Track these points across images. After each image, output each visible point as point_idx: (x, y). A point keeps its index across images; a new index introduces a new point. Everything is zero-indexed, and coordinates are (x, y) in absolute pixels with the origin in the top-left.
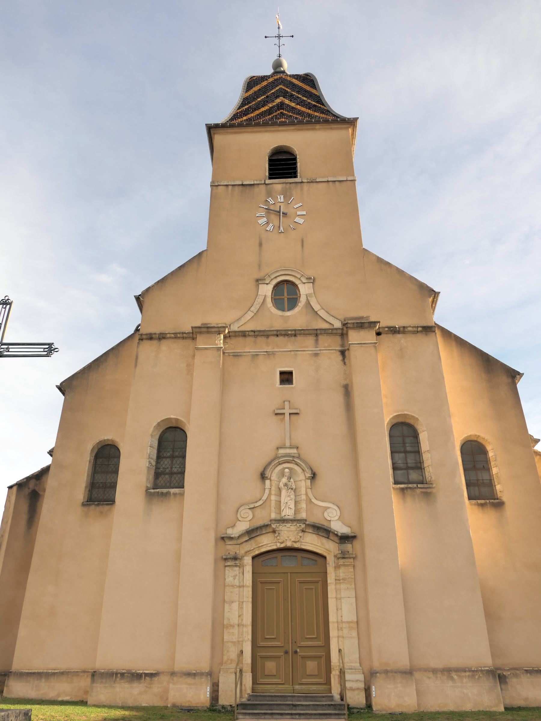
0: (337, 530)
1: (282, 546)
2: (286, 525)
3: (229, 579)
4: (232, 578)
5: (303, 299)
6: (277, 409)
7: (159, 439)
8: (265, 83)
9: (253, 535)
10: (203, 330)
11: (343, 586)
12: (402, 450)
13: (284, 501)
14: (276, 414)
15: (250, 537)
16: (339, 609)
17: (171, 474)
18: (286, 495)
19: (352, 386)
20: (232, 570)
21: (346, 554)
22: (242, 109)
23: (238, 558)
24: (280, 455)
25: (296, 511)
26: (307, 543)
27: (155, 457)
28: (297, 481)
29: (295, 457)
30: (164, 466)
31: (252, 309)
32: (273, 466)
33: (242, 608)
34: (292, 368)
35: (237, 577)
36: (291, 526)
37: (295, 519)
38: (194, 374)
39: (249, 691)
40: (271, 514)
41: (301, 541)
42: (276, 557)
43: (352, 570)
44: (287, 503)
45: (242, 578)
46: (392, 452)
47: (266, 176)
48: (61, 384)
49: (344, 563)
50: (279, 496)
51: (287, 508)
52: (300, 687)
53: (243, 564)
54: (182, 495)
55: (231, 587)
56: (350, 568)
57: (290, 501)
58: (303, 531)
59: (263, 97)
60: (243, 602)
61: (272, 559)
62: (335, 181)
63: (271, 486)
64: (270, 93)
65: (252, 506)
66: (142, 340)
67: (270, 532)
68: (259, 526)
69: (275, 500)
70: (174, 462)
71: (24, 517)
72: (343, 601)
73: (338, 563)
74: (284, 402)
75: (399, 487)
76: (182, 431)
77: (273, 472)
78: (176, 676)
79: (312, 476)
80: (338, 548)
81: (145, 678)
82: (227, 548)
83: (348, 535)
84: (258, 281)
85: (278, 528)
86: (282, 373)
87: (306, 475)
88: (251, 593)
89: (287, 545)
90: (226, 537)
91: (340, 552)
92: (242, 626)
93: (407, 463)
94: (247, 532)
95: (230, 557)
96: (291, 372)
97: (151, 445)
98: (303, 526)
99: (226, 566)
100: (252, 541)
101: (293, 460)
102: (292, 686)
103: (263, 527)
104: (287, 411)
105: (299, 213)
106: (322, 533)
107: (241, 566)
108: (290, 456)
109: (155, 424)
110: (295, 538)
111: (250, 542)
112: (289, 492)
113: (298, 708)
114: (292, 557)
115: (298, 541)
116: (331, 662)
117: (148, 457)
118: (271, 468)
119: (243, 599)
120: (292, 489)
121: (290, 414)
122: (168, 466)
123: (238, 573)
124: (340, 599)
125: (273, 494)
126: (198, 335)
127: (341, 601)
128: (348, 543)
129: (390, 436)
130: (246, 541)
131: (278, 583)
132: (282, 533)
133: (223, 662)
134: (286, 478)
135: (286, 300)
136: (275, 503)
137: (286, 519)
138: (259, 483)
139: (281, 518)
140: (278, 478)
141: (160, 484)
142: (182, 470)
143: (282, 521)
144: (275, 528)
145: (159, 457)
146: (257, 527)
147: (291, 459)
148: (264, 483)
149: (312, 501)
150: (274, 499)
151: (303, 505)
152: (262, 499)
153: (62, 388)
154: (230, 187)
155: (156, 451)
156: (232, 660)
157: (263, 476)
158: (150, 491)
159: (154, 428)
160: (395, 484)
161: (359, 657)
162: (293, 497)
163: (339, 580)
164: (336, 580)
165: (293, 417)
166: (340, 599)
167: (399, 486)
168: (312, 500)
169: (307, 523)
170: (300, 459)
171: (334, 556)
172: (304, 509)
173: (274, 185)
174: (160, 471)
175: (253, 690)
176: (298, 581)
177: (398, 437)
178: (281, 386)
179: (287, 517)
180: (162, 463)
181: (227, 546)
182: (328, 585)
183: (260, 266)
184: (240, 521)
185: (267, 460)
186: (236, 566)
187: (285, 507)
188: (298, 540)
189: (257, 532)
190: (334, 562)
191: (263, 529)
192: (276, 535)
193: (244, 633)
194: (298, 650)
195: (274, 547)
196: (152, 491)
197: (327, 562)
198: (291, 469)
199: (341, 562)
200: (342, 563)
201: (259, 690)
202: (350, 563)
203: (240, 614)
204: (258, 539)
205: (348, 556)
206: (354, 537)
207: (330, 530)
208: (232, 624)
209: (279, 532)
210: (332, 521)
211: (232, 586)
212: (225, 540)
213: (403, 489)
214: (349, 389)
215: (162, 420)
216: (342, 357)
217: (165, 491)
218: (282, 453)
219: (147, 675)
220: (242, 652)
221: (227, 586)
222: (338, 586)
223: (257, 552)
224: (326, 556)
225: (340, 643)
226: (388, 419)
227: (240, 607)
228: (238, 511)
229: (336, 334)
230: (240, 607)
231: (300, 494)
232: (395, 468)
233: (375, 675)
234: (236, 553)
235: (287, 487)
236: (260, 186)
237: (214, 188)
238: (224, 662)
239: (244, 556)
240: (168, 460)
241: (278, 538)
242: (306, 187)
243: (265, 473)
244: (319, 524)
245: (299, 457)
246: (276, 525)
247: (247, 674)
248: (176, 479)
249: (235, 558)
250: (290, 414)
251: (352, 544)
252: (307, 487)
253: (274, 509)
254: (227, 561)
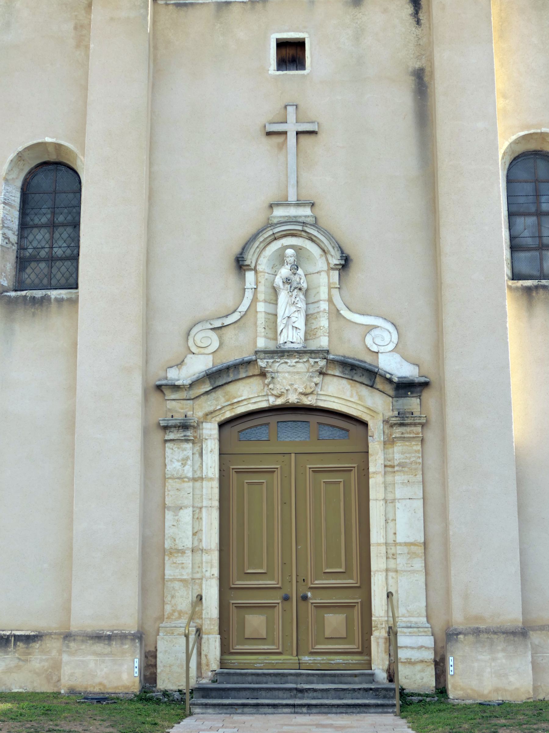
0: (390, 372)
1: (279, 402)
2: (286, 360)
3: (174, 465)
4: (180, 464)
6: (270, 123)
7: (22, 189)
11: (399, 478)
12: (533, 209)
13: (282, 314)
14: (269, 134)
15: (214, 386)
16: (389, 521)
17: (51, 259)
18: (287, 303)
19: (432, 73)
20: (178, 448)
21: (407, 417)
23: (191, 426)
24: (275, 221)
25: (309, 335)
26: (330, 396)
27: (15, 225)
28: (310, 274)
29: (308, 224)
30: (35, 244)
32: (261, 242)
33: (200, 519)
34: (303, 32)
35: (189, 462)
36: (296, 362)
37: (305, 349)
38: (92, 46)
39: (215, 666)
40: (258, 341)
41: (317, 392)
42: (268, 424)
43: (419, 448)
44: (289, 317)
45: (199, 463)
46: (511, 215)
49: (403, 433)
50: (273, 303)
51: (290, 327)
52: (312, 659)
53: (200, 436)
54: (74, 302)
55: (176, 480)
56: (413, 443)
57: (296, 314)
58: (321, 373)
60: (201, 508)
61: (259, 427)
63: (257, 284)
65: (218, 324)
67: (254, 376)
68: (231, 363)
69: (265, 312)
70: (57, 235)
72: (398, 505)
73: (391, 435)
74: (286, 107)
75: (522, 285)
76: (71, 172)
77: (262, 256)
78: (74, 640)
79: (343, 262)
80: (392, 407)
81: (15, 644)
82: (168, 407)
83: (414, 380)
85: (270, 367)
86: (281, 45)
87: (330, 261)
88: (216, 491)
89: (288, 399)
90: (166, 385)
91: (396, 413)
92: (200, 552)
93: (540, 237)
94: (207, 375)
95: (174, 424)
96: (301, 41)
97: (5, 199)
98: (322, 363)
99: (166, 441)
100: (219, 393)
101: (303, 231)
102: (297, 658)
103: (241, 366)
104: (291, 128)
106: (360, 376)
107: (198, 441)
108: (297, 222)
110: (306, 386)
111: (213, 395)
112: (294, 296)
113: (306, 694)
114: (299, 423)
115: (312, 393)
116: (373, 616)
117: (2, 225)
118: (258, 247)
119: (202, 502)
120: (300, 289)
121: (298, 133)
122: (43, 243)
123: (190, 454)
124: (392, 502)
125: (261, 300)
127: (395, 506)
128: (413, 397)
129: (510, 181)
130: (207, 393)
131: (271, 472)
132: (280, 378)
133: (164, 615)
134: (289, 267)
136: (265, 318)
137: (287, 349)
138: (232, 279)
139: (277, 348)
140: (272, 268)
141: (28, 281)
142: (72, 252)
143: (279, 354)
144: (265, 368)
145: (24, 226)
146: (229, 366)
147: (300, 228)
148: (243, 278)
149: (341, 314)
150: (263, 310)
151: (324, 322)
152: (239, 310)
155: (16, 214)
156: (180, 613)
157: (241, 263)
158: (8, 294)
159: (10, 163)
160: (513, 280)
161: (427, 606)
162: (302, 305)
163: (393, 467)
164: (385, 466)
165: (304, 139)
166: (393, 501)
167: (521, 283)
168: (342, 312)
169: (331, 357)
170: (317, 227)
171: (384, 421)
172: (324, 329)
174: (28, 254)
175: (222, 664)
176: (310, 468)
177: (526, 182)
178: (280, 72)
179: (289, 346)
180: (31, 237)
181: (168, 402)
182: (370, 476)
184: (194, 353)
185: (251, 230)
186: (187, 441)
187: (286, 325)
188: (312, 389)
189: (229, 376)
190: (384, 432)
191: (241, 370)
192: (267, 381)
193: (204, 564)
194: (309, 594)
195: (264, 405)
196: (13, 294)
197: (370, 433)
198: (298, 249)
199: (397, 432)
200: (398, 435)
201: (234, 663)
202: (416, 434)
203: (195, 531)
204: (231, 388)
205: (412, 421)
206: (425, 385)
207: (376, 370)
208: (180, 548)
209: (273, 376)
210: (382, 353)
211: (178, 478)
212: (164, 390)
213: (528, 290)
214: (426, 79)
215: (26, 148)
216: (412, 9)
217: (38, 294)
218: (281, 217)
219: (18, 638)
220: (200, 598)
221: (168, 478)
222: (389, 478)
223: (228, 414)
224: (367, 421)
225: (391, 581)
226: (507, 144)
227: (196, 516)
228: (188, 334)
230: (196, 516)
231: (316, 300)
232: (514, 248)
233: (455, 637)
234: (186, 416)
235: (289, 286)
238: (166, 616)
239: (202, 423)
240: (43, 231)
241: (271, 386)
243: (245, 256)
244: (354, 359)
245: (315, 225)
246: (267, 362)
247: (210, 636)
248: (61, 269)
249: (185, 426)
250: (298, 133)
251: (420, 399)
252: (332, 286)
253: (263, 330)
254: (168, 431)
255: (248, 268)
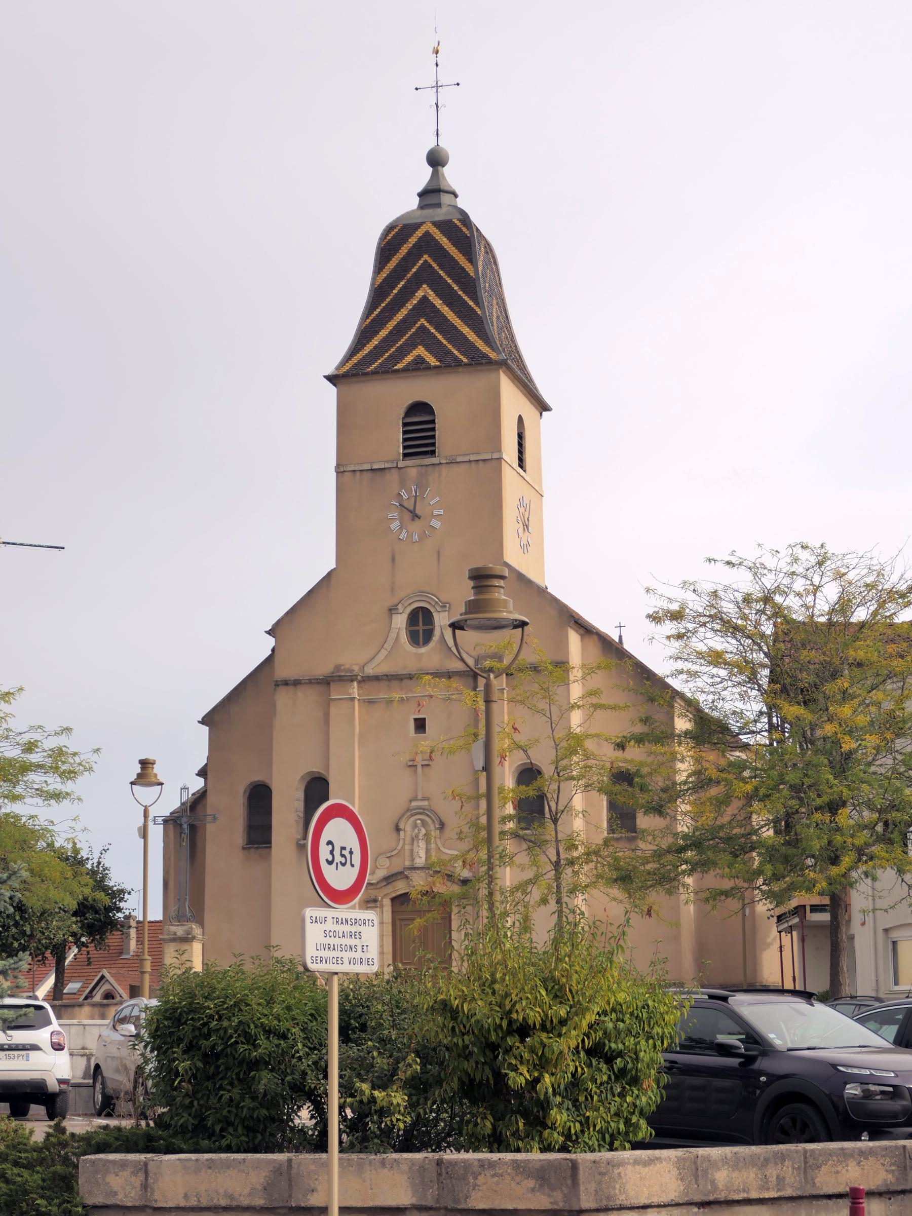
5: (437, 632)
8: (404, 250)
9: (390, 881)
10: (335, 678)
14: (410, 766)
22: (373, 315)
24: (411, 808)
31: (385, 646)
47: (399, 453)
48: (203, 718)
59: (402, 283)
62: (478, 461)
64: (411, 273)
65: (388, 855)
66: (278, 685)
71: (186, 852)
84: (392, 610)
86: (415, 720)
100: (390, 886)
105: (436, 512)
107: (382, 906)
108: (421, 809)
109: (299, 777)
126: (332, 684)
135: (421, 632)
148: (399, 834)
151: (433, 853)
153: (203, 722)
154: (358, 474)
165: (425, 768)
173: (408, 469)
179: (417, 865)
183: (393, 589)
198: (421, 820)
204: (394, 883)
223: (394, 895)
229: (468, 675)
236: (393, 470)
237: (340, 474)
242: (444, 470)
249: (375, 901)
255: (401, 829)
